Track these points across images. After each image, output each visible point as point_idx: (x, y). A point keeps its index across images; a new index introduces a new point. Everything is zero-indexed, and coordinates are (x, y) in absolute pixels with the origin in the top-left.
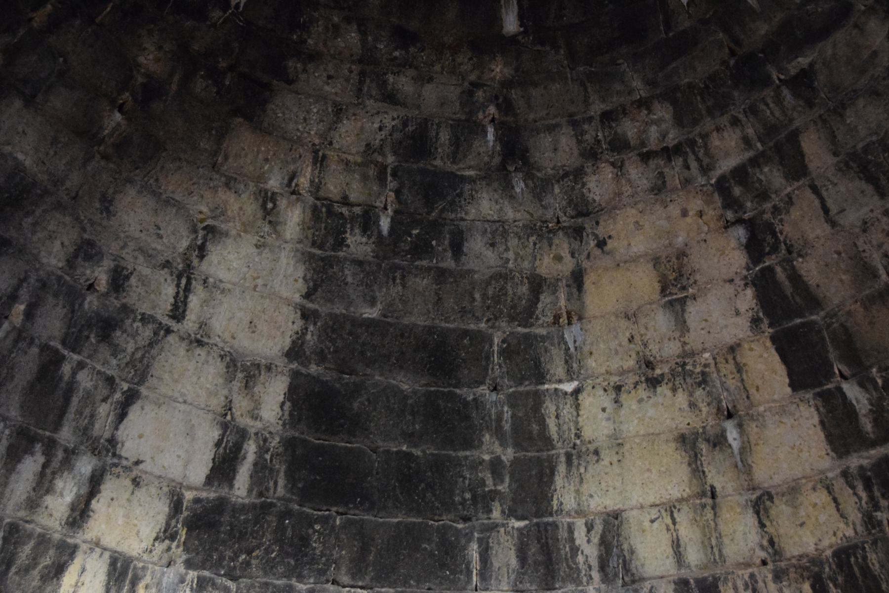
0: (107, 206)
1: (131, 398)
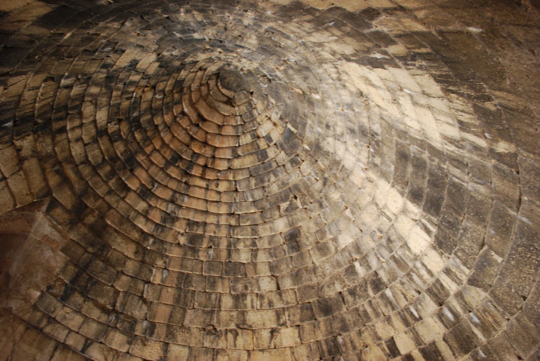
0: (363, 224)
1: (406, 244)
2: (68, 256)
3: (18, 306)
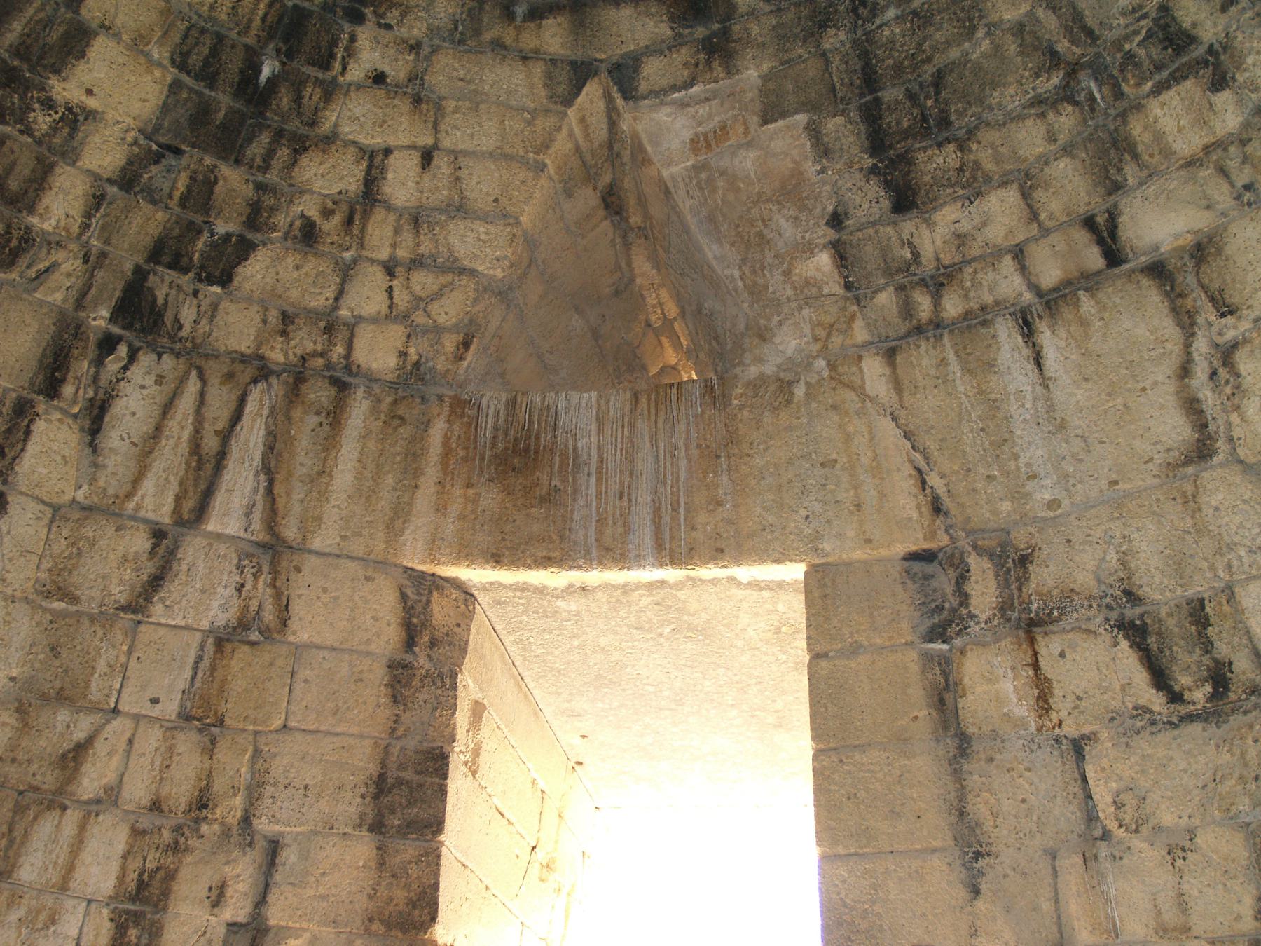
2: (797, 112)
3: (807, 331)
